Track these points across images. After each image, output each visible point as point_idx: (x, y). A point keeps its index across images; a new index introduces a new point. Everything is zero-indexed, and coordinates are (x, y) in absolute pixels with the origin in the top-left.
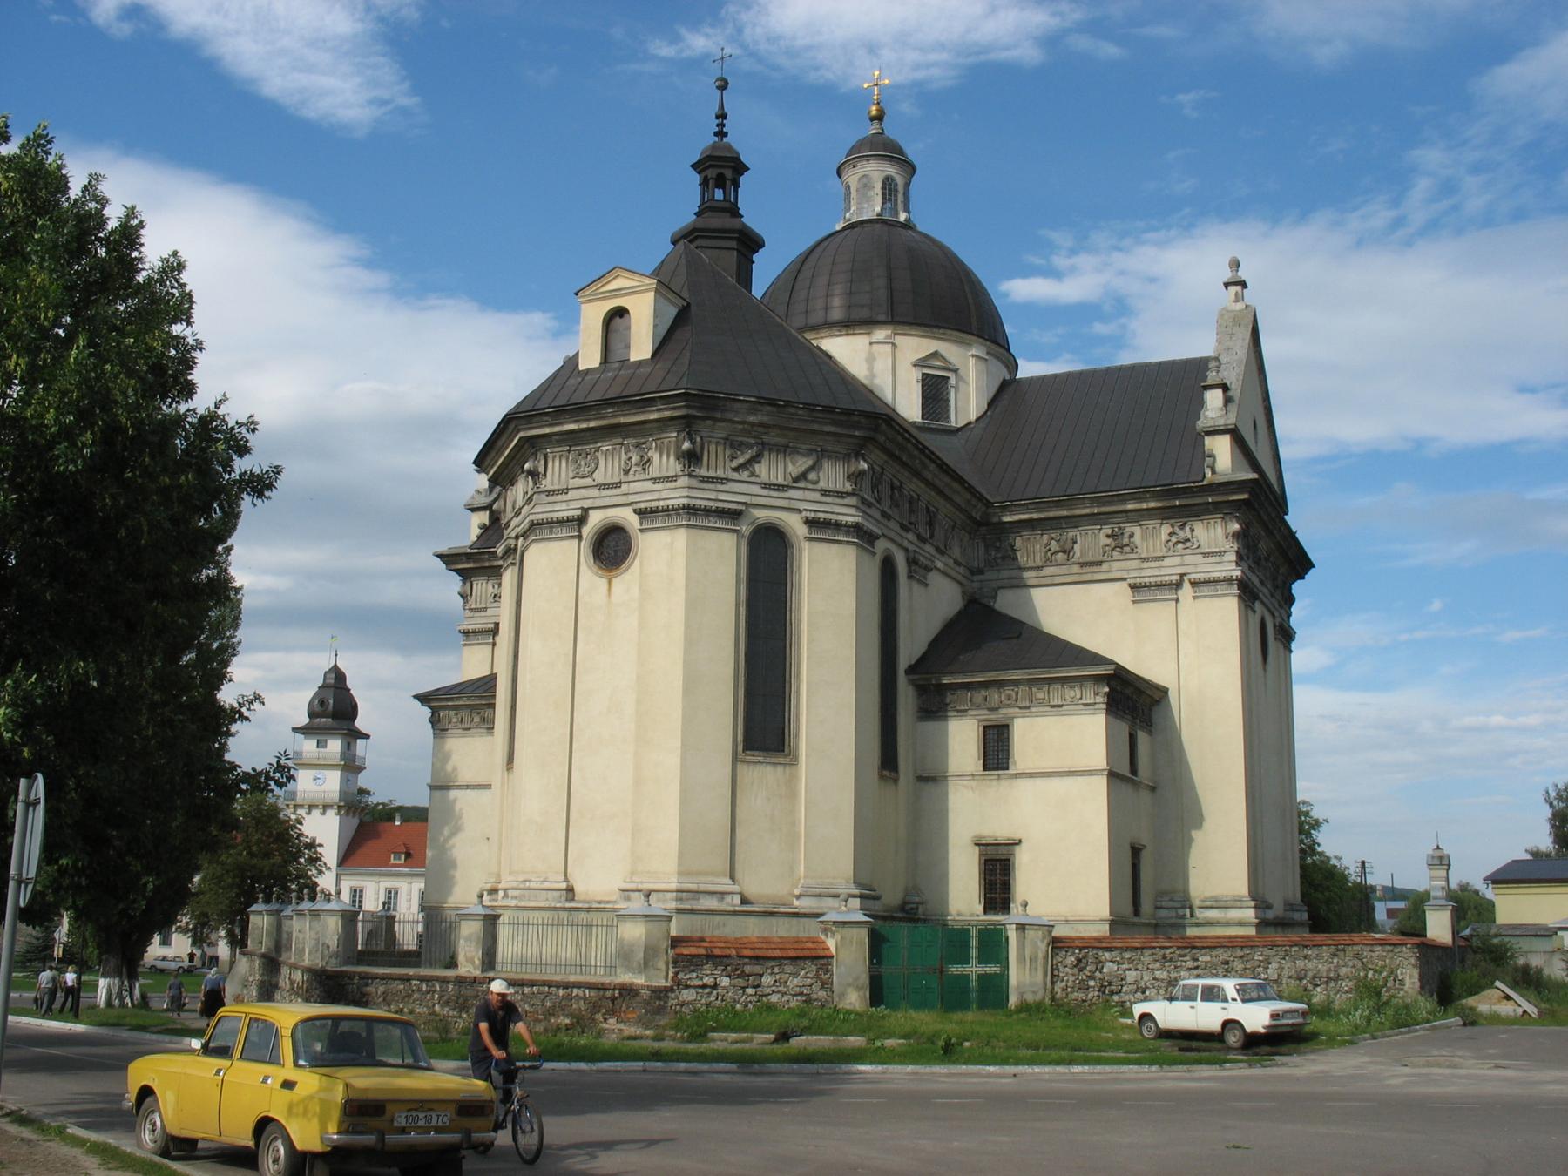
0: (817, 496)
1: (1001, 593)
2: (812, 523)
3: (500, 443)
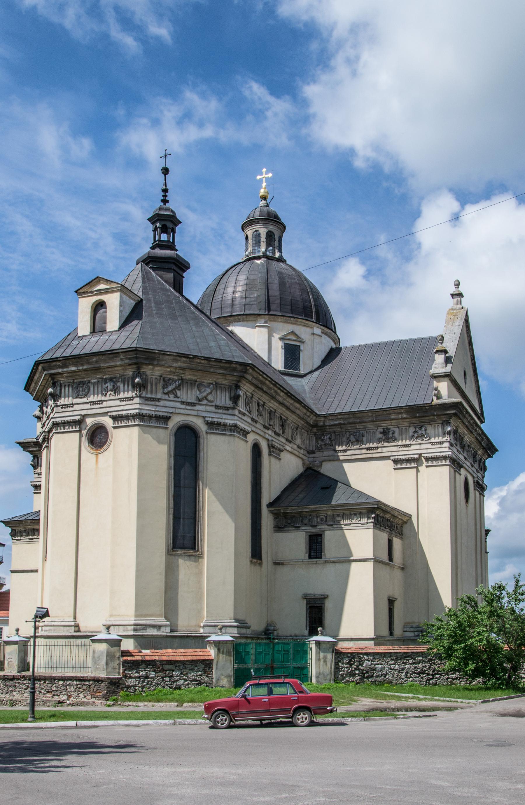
0: (213, 409)
1: (324, 464)
2: (211, 424)
3: (36, 378)
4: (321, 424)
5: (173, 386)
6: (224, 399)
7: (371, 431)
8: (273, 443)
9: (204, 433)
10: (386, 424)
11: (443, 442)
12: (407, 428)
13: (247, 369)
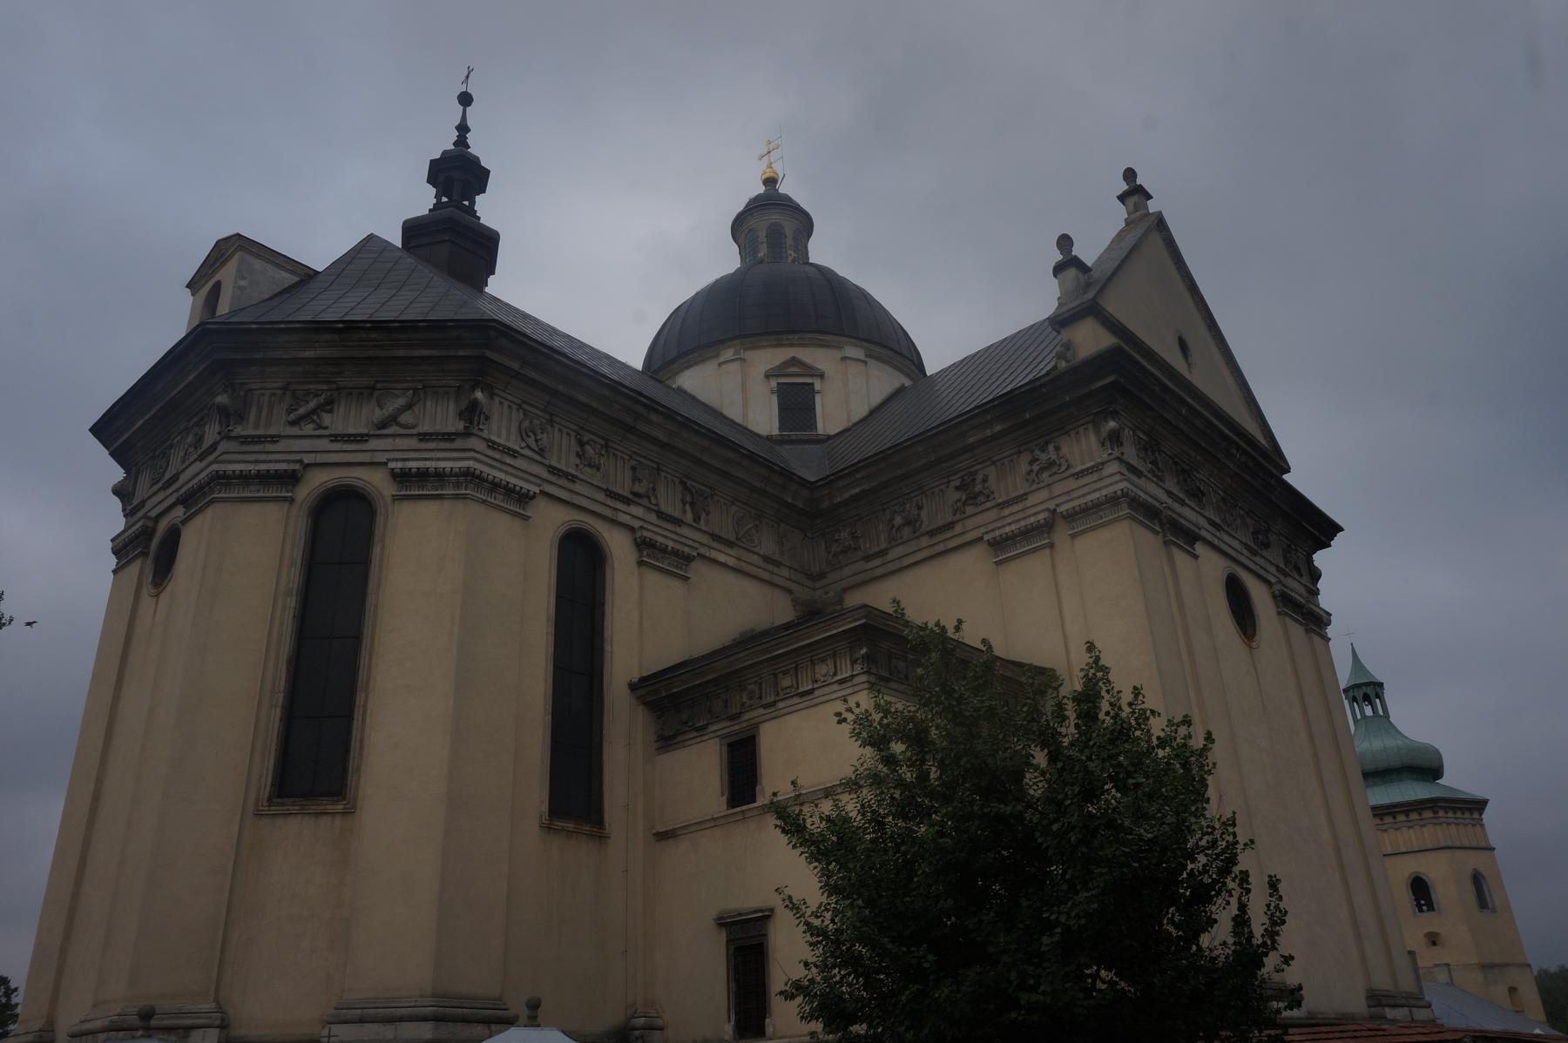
0: (413, 443)
4: (826, 504)
5: (313, 404)
8: (645, 533)
9: (389, 500)
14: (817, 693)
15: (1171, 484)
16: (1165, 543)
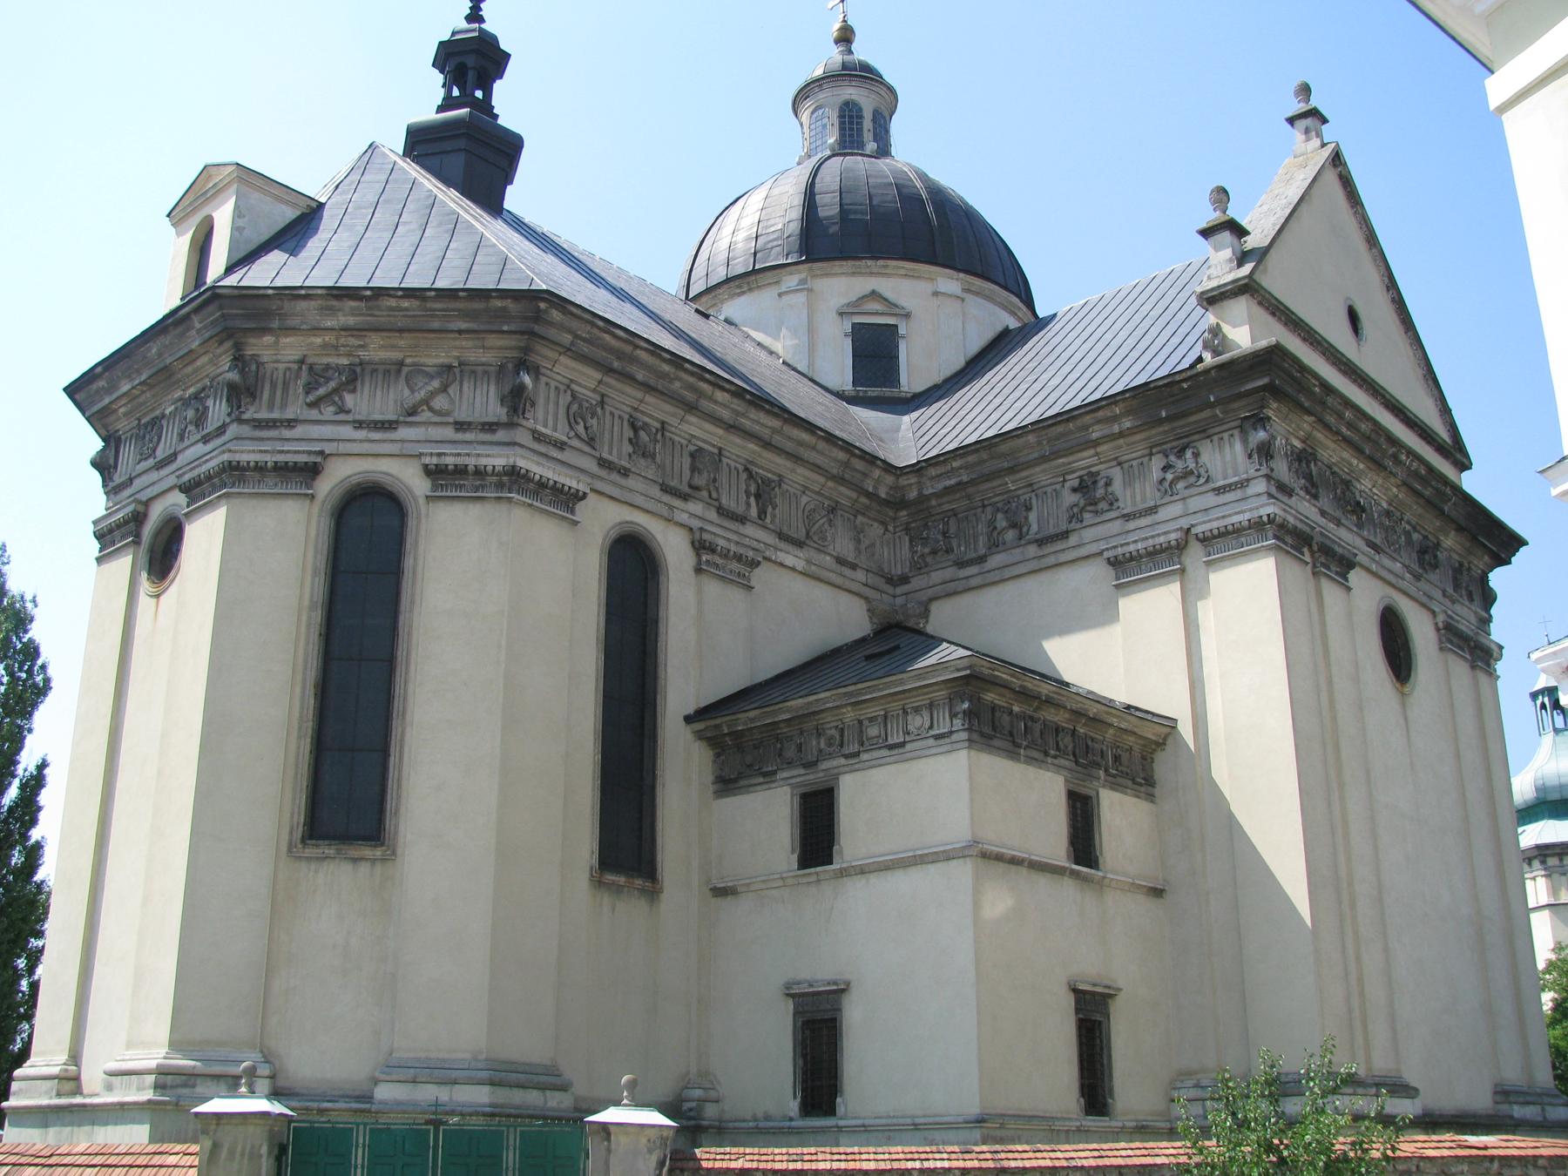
0: (449, 433)
2: (436, 473)
4: (913, 494)
5: (332, 384)
6: (484, 402)
7: (1049, 489)
8: (705, 536)
9: (422, 501)
10: (1084, 461)
11: (1248, 480)
12: (1145, 460)
13: (539, 310)
14: (908, 747)
15: (1325, 501)
16: (1314, 574)
